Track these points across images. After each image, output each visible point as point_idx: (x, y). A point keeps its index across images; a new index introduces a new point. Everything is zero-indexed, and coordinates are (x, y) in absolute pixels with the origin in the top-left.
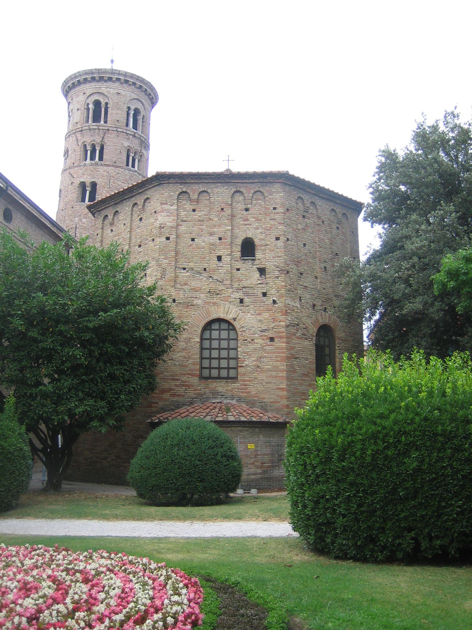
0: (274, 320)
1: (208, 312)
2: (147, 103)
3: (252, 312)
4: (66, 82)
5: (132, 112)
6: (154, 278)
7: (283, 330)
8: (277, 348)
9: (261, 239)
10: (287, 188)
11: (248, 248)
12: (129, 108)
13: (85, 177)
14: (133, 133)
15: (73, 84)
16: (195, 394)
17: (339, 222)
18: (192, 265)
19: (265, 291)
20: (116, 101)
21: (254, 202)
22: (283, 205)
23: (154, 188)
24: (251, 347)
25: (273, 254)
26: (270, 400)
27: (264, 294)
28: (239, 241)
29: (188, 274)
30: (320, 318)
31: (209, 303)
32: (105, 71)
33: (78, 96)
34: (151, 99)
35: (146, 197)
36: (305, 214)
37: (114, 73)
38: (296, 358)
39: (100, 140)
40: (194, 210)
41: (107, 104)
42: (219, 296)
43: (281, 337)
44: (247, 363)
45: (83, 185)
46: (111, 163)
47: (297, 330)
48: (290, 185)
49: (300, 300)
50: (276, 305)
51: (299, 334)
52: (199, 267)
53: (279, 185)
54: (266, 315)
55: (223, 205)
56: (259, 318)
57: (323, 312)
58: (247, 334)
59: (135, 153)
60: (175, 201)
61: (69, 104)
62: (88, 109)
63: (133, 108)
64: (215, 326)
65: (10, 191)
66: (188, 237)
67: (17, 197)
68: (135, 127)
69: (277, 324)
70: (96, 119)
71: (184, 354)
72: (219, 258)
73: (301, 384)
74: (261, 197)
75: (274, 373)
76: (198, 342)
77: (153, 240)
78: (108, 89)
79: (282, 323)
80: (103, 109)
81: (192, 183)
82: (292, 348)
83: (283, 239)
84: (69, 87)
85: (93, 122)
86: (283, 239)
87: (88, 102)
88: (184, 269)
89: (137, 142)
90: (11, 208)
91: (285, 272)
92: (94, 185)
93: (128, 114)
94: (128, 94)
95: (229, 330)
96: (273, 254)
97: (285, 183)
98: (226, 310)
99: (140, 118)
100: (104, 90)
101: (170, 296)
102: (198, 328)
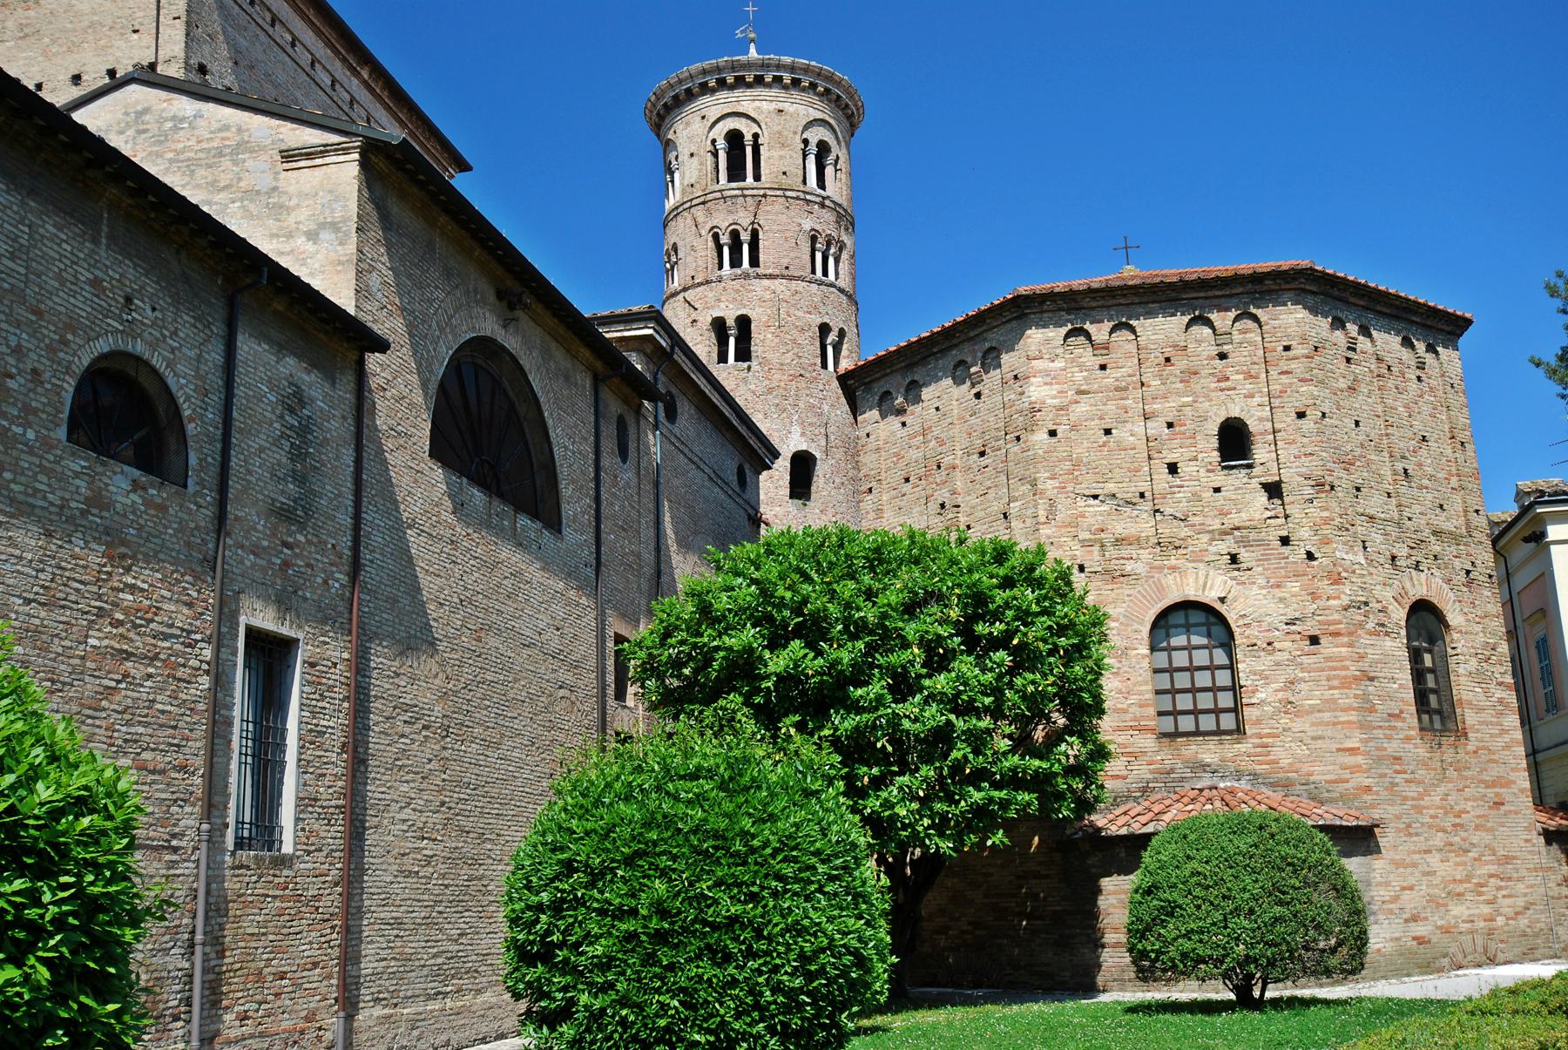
0: (1314, 596)
1: (1161, 589)
3: (1261, 581)
5: (813, 148)
6: (1029, 521)
7: (1336, 617)
8: (1328, 659)
9: (1261, 419)
10: (1310, 300)
11: (1234, 442)
12: (806, 142)
13: (722, 305)
14: (818, 200)
15: (676, 97)
16: (1152, 772)
17: (1421, 366)
18: (1111, 487)
19: (1285, 533)
20: (776, 128)
21: (1237, 337)
22: (1304, 340)
23: (1008, 326)
24: (1265, 662)
25: (1294, 450)
26: (1328, 777)
27: (1285, 541)
28: (1213, 428)
29: (1105, 508)
31: (1161, 568)
32: (749, 66)
33: (688, 124)
34: (850, 117)
35: (987, 345)
36: (1350, 354)
37: (768, 66)
38: (1372, 679)
39: (749, 221)
40: (1103, 367)
41: (756, 136)
42: (1181, 551)
43: (1336, 634)
44: (1262, 696)
45: (719, 325)
46: (777, 272)
48: (1313, 293)
50: (1315, 563)
51: (1370, 626)
52: (1129, 490)
53: (1291, 294)
54: (1294, 587)
55: (1169, 352)
56: (1278, 593)
58: (1253, 632)
59: (829, 244)
60: (1060, 351)
63: (813, 142)
64: (1179, 618)
65: (679, 357)
66: (1096, 427)
67: (687, 366)
68: (821, 183)
69: (1322, 603)
70: (736, 172)
71: (1117, 684)
72: (1173, 468)
73: (1389, 738)
74: (1250, 324)
75: (1327, 716)
76: (1144, 656)
77: (1018, 438)
78: (757, 103)
79: (1332, 602)
80: (749, 150)
81: (1093, 309)
82: (1362, 657)
83: (1314, 415)
84: (665, 105)
85: (730, 181)
86: (1314, 415)
87: (711, 136)
88: (1095, 497)
89: (829, 216)
90: (674, 391)
91: (1327, 488)
92: (744, 323)
95: (1208, 625)
96: (1294, 450)
97: (1304, 291)
98: (1201, 582)
99: (831, 159)
100: (747, 107)
101: (1073, 557)
102: (1142, 623)
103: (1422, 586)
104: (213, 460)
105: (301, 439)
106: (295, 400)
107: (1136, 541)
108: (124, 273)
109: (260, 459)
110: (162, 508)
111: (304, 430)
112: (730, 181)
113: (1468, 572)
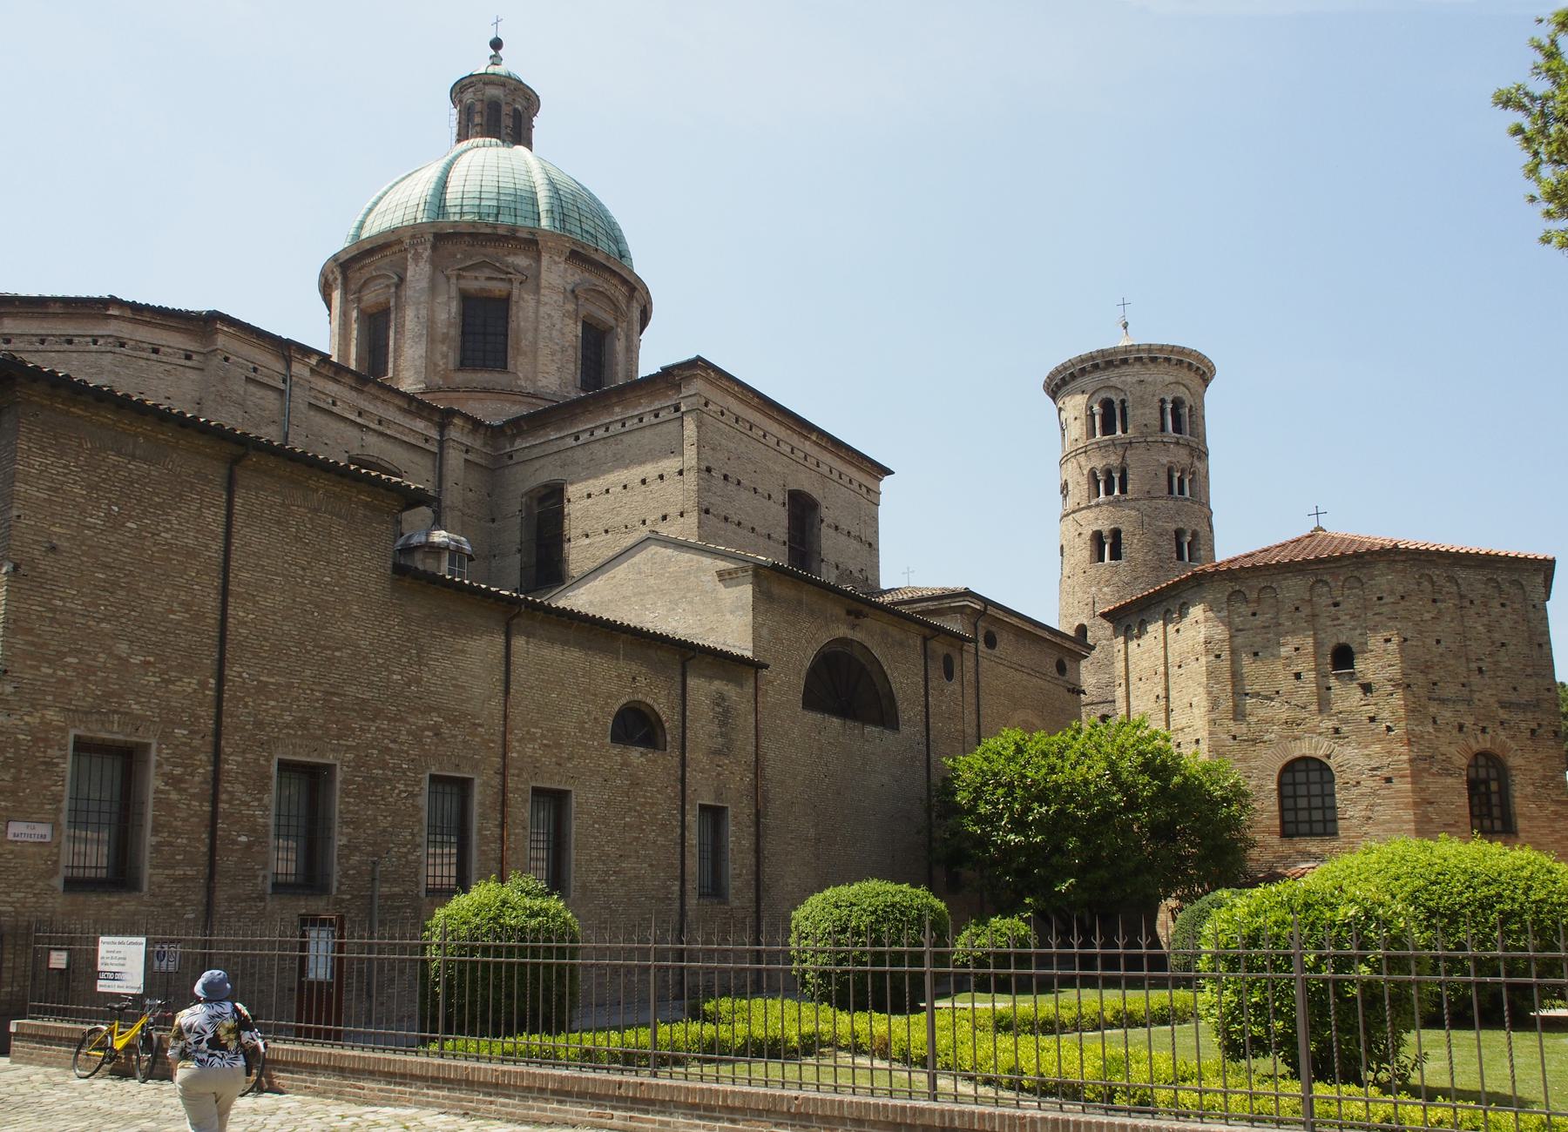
2: (1195, 381)
4: (1051, 378)
12: (1163, 401)
18: (1256, 688)
27: (1372, 719)
30: (1472, 741)
41: (1123, 402)
47: (1431, 764)
49: (1435, 722)
54: (1377, 748)
57: (1480, 736)
61: (1060, 410)
62: (1093, 416)
63: (1169, 399)
68: (1178, 428)
70: (1108, 428)
72: (1298, 676)
85: (1104, 434)
93: (1162, 411)
94: (1159, 378)
100: (1115, 381)
103: (1484, 743)
104: (678, 737)
105: (725, 715)
106: (720, 699)
107: (1272, 722)
108: (628, 668)
109: (702, 730)
110: (655, 761)
111: (726, 711)
112: (1104, 434)
113: (1533, 731)
